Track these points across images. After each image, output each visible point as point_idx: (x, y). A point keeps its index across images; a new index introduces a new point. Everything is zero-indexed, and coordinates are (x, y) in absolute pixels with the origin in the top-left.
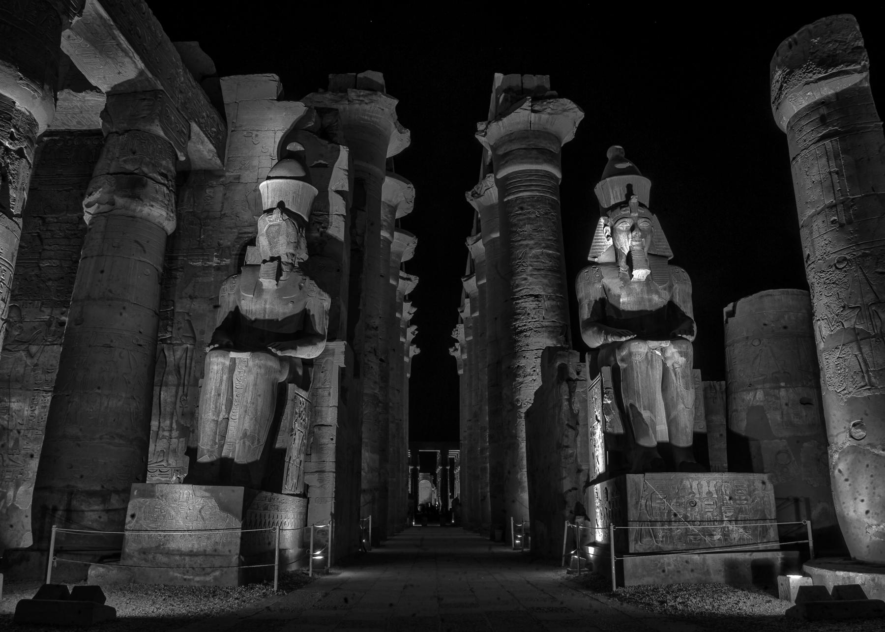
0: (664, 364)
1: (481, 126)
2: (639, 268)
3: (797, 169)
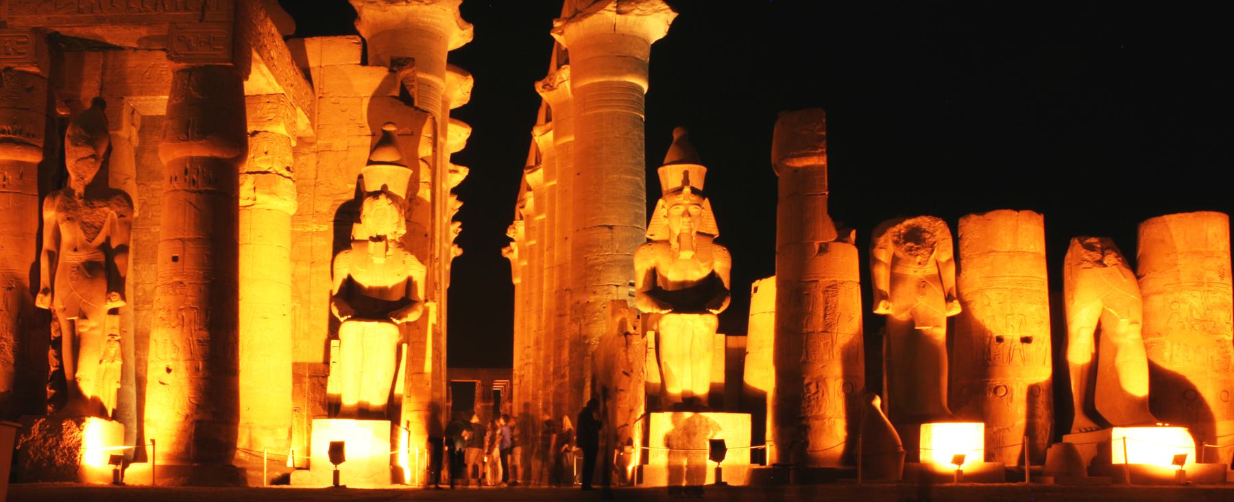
1: (557, 24)
3: (779, 208)
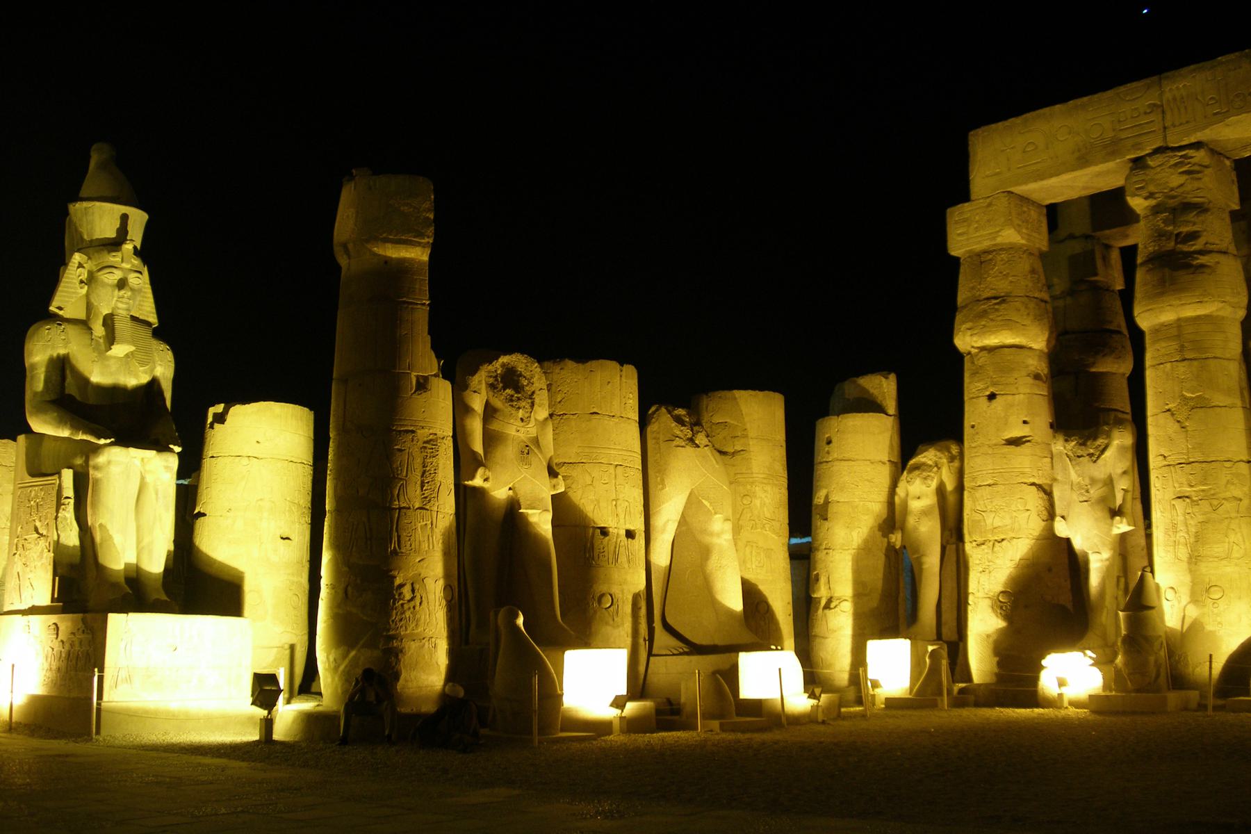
0: (143, 478)
2: (123, 342)
